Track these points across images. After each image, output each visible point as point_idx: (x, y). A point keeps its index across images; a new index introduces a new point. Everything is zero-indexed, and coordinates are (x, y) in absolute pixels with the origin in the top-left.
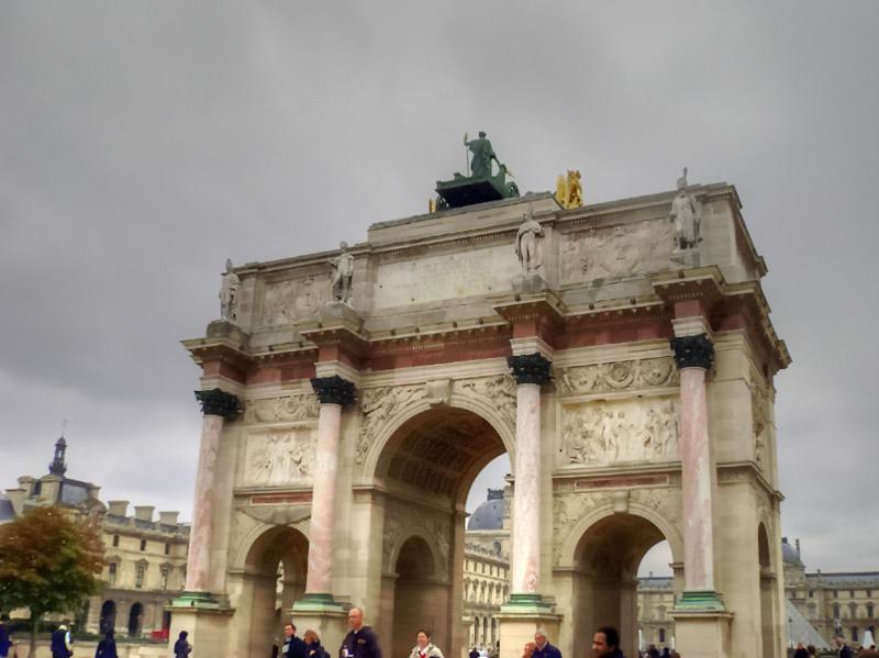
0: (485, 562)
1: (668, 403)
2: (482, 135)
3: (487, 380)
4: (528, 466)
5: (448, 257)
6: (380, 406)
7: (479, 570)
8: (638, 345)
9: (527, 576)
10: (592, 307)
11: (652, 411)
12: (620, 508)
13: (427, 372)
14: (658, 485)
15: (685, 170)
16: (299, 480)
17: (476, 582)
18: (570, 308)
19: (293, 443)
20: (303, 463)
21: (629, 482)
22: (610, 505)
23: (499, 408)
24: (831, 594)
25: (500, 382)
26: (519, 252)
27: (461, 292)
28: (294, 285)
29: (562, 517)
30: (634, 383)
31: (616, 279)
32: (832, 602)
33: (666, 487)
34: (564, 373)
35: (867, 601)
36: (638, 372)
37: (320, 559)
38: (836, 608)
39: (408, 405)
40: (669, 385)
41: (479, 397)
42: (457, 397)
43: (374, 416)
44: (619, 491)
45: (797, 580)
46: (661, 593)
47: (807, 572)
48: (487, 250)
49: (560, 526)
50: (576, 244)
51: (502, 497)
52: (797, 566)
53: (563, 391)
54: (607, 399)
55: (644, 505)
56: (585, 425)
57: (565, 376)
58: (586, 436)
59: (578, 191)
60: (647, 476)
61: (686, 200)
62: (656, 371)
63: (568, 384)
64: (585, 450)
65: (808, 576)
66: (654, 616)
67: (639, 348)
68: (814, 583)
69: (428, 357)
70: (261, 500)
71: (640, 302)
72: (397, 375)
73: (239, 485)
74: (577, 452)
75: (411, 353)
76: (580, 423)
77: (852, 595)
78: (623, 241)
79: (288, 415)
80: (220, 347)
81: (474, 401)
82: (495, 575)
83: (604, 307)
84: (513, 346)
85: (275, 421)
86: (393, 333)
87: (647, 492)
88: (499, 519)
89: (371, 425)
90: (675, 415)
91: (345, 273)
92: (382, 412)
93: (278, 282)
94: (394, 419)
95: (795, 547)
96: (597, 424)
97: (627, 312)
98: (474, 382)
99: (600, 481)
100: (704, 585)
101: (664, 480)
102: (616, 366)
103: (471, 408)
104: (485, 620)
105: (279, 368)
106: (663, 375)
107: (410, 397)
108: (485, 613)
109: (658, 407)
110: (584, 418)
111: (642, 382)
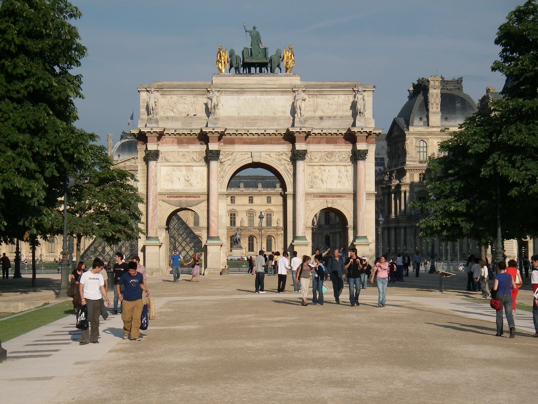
3: (276, 153)
5: (253, 97)
9: (302, 230)
12: (330, 206)
13: (250, 147)
16: (190, 188)
20: (192, 181)
21: (333, 197)
25: (282, 154)
27: (261, 113)
28: (175, 98)
29: (308, 208)
33: (346, 199)
36: (337, 156)
39: (241, 160)
40: (348, 162)
42: (264, 159)
43: (227, 164)
44: (330, 199)
50: (311, 100)
56: (315, 173)
57: (309, 155)
58: (316, 177)
62: (344, 156)
69: (251, 140)
70: (171, 197)
71: (340, 131)
72: (236, 147)
76: (313, 172)
78: (330, 102)
79: (181, 160)
83: (327, 131)
87: (339, 200)
89: (225, 167)
91: (216, 103)
92: (230, 162)
94: (235, 166)
98: (270, 153)
99: (322, 196)
101: (346, 196)
106: (346, 158)
107: (242, 157)
109: (343, 169)
110: (315, 171)
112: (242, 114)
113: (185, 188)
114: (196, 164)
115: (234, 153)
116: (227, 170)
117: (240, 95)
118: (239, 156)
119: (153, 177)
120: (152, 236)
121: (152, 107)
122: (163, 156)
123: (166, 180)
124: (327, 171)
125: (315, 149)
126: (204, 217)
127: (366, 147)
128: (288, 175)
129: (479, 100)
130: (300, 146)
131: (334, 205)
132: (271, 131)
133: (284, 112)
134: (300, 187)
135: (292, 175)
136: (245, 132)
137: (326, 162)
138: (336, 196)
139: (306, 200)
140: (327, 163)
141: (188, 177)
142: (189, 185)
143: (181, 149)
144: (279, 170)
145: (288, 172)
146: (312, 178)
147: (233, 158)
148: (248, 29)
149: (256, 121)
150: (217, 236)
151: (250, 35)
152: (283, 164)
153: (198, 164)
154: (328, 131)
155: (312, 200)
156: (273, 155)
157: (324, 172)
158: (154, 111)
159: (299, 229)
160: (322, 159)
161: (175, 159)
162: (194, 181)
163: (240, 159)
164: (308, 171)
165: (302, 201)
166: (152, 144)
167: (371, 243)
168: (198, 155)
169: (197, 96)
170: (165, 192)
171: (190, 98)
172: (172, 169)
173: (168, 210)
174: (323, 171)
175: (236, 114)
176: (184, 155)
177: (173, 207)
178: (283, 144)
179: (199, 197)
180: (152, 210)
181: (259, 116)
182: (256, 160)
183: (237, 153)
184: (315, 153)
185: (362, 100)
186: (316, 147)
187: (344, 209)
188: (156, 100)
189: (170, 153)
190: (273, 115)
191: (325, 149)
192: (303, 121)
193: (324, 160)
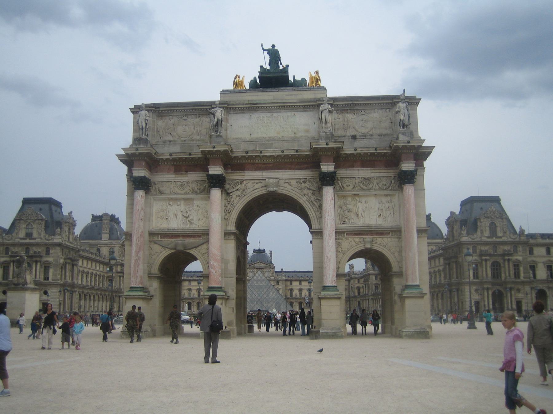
0: (93, 260)
1: (389, 198)
2: (273, 46)
4: (331, 225)
6: (237, 190)
7: (89, 266)
8: (374, 170)
10: (355, 150)
11: (381, 201)
12: (368, 246)
13: (264, 174)
14: (386, 236)
15: (404, 90)
16: (188, 226)
17: (88, 273)
18: (344, 149)
19: (182, 206)
20: (191, 217)
22: (363, 245)
23: (304, 195)
24: (289, 283)
25: (305, 182)
26: (321, 120)
28: (174, 120)
29: (340, 250)
30: (373, 188)
31: (363, 136)
32: (289, 288)
33: (389, 237)
34: (338, 180)
36: (375, 183)
37: (217, 269)
38: (291, 291)
39: (253, 190)
40: (391, 190)
41: (293, 188)
42: (282, 188)
43: (234, 195)
44: (368, 238)
45: (270, 275)
46: (190, 281)
47: (276, 269)
48: (293, 113)
49: (339, 253)
50: (340, 116)
51: (101, 220)
52: (270, 266)
53: (338, 188)
54: (360, 194)
55: (380, 245)
57: (339, 182)
58: (349, 211)
59: (319, 81)
60: (380, 232)
61: (404, 105)
62: (384, 183)
63: (341, 186)
64: (349, 218)
65: (276, 272)
66: (184, 294)
67: (376, 171)
68: (279, 277)
71: (379, 150)
72: (246, 174)
73: (151, 228)
74: (345, 218)
75: (254, 164)
76: (346, 204)
77: (300, 284)
78: (365, 117)
79: (179, 191)
80: (147, 153)
81: (291, 191)
82: (98, 268)
84: (322, 167)
85: (171, 194)
86: (247, 153)
87: (381, 239)
88: (100, 234)
89: (233, 199)
90: (393, 204)
91: (220, 118)
92: (238, 193)
93: (166, 116)
94: (246, 197)
95: (269, 255)
96: (354, 206)
97: (372, 154)
98: (290, 181)
100: (417, 282)
101: (388, 234)
102: (365, 178)
103: (289, 194)
104: (102, 296)
105: (172, 165)
106: (388, 185)
107: (254, 186)
108: (85, 291)
109: (384, 199)
110: (348, 202)
111: (377, 187)
112: (255, 136)
113: (183, 226)
114: (196, 196)
115: (244, 182)
116: (235, 202)
117: (252, 113)
118: (250, 185)
119: (139, 210)
120: (134, 286)
121: (142, 126)
122: (157, 187)
123: (160, 216)
124: (363, 202)
125: (347, 174)
126: (205, 263)
127: (414, 168)
128: (312, 208)
129: (446, 219)
130: (327, 167)
131: (373, 245)
132: (290, 152)
133: (307, 131)
134: (328, 219)
135: (318, 207)
136: (257, 154)
137: (362, 191)
138: (376, 233)
139: (336, 239)
140: (363, 192)
141: (187, 212)
142: (188, 222)
143: (179, 178)
144: (301, 202)
145: (313, 203)
146: (343, 211)
147: (242, 188)
148: (265, 48)
149: (272, 142)
150: (218, 286)
151: (268, 54)
152: (307, 193)
154: (363, 150)
155: (345, 239)
156: (293, 182)
157: (360, 203)
158: (144, 130)
159: (328, 276)
160: (357, 186)
161: (171, 190)
162: (194, 216)
163: (252, 189)
164: (339, 203)
165: (331, 239)
166: (139, 170)
167: (426, 294)
168: (199, 185)
169: (200, 116)
170: (157, 231)
171: (192, 120)
172: (168, 203)
173: (161, 254)
174: (358, 202)
175: (248, 136)
176: (181, 186)
177: (166, 251)
178: (306, 168)
179: (200, 237)
180: (136, 251)
181: (276, 137)
182: (271, 189)
183: (248, 181)
184: (348, 179)
185: (405, 109)
186: (348, 172)
187: (386, 250)
188: (147, 118)
189: (165, 183)
190: (293, 135)
191: (360, 174)
192: (330, 136)
193: (359, 187)
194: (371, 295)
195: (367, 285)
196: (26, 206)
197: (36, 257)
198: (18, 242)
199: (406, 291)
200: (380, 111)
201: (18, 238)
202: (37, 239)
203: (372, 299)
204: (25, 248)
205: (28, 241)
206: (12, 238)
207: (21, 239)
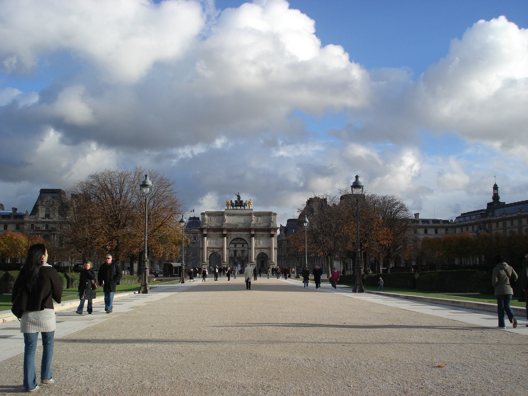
35: (235, 249)
92: (230, 237)
109: (267, 240)
133: (248, 221)
153: (220, 238)
156: (244, 235)
176: (215, 235)
178: (247, 232)
194: (283, 256)
195: (280, 248)
196: (43, 194)
197: (53, 231)
198: (40, 220)
199: (271, 263)
200: (267, 216)
201: (40, 218)
202: (53, 219)
203: (284, 259)
204: (45, 224)
205: (47, 220)
206: (35, 218)
207: (42, 218)
